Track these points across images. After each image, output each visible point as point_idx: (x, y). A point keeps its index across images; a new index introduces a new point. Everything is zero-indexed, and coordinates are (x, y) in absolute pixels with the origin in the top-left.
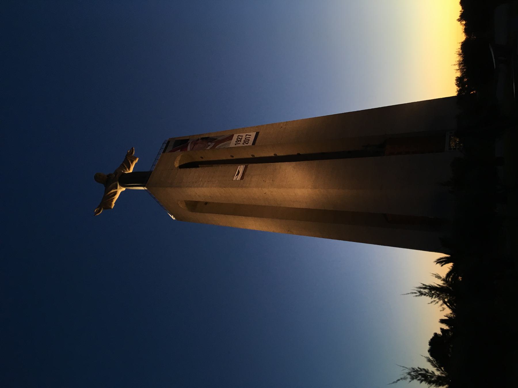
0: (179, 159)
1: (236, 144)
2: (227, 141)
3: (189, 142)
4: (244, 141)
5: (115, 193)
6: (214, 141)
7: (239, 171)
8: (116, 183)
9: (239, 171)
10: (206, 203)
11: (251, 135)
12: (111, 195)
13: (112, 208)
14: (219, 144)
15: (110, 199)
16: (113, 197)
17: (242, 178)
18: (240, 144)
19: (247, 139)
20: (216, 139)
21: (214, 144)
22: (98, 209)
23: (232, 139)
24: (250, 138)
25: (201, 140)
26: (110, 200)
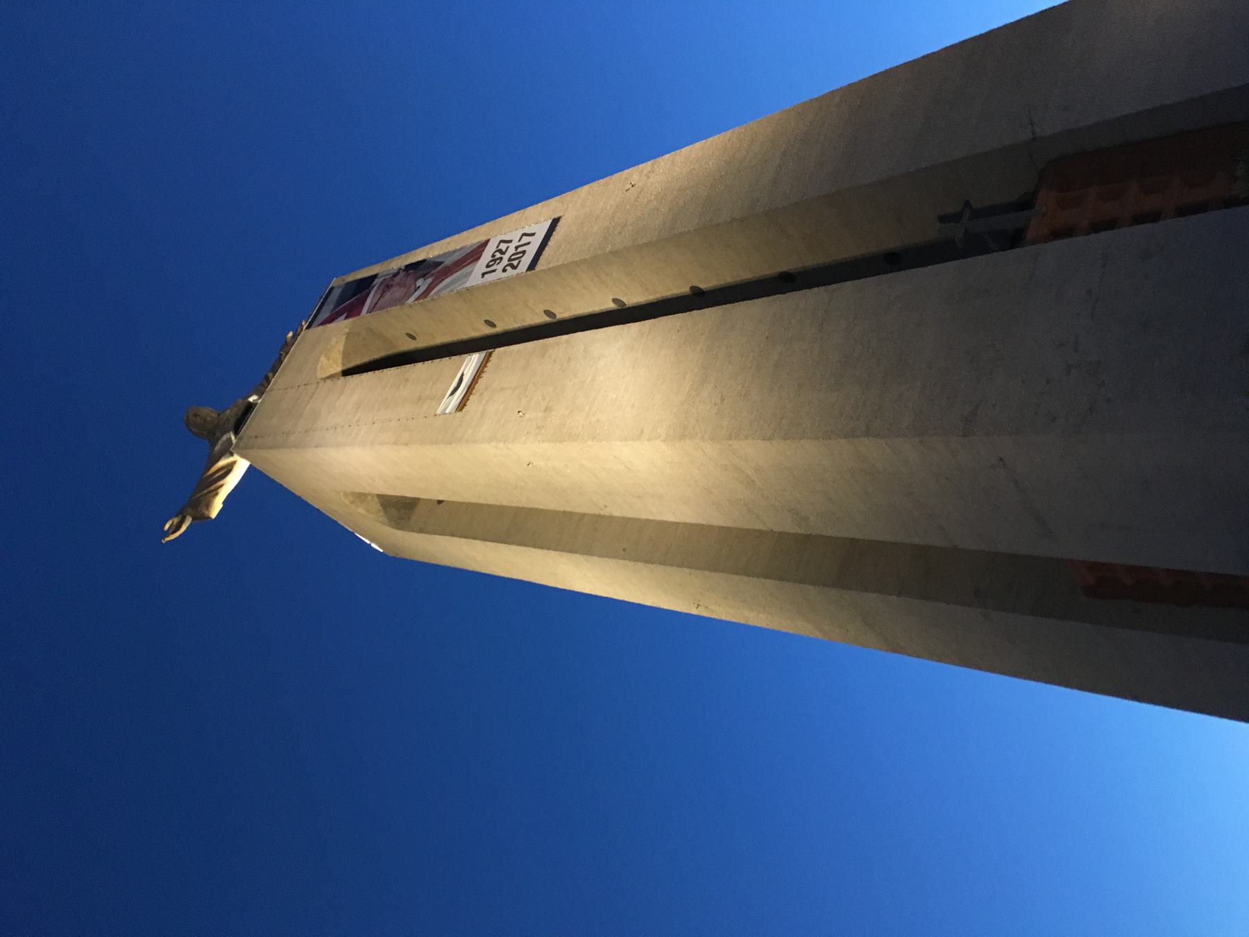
0: (341, 347)
1: (483, 275)
2: (463, 268)
3: (373, 285)
4: (510, 260)
5: (228, 469)
6: (433, 272)
7: (463, 375)
8: (225, 438)
9: (463, 375)
10: (440, 502)
11: (533, 234)
12: (217, 475)
13: (214, 513)
14: (443, 280)
15: (212, 488)
16: (221, 482)
17: (461, 406)
18: (494, 271)
19: (520, 250)
20: (442, 263)
21: (429, 280)
22: (176, 520)
23: (479, 258)
24: (529, 243)
25: (404, 273)
26: (213, 491)
